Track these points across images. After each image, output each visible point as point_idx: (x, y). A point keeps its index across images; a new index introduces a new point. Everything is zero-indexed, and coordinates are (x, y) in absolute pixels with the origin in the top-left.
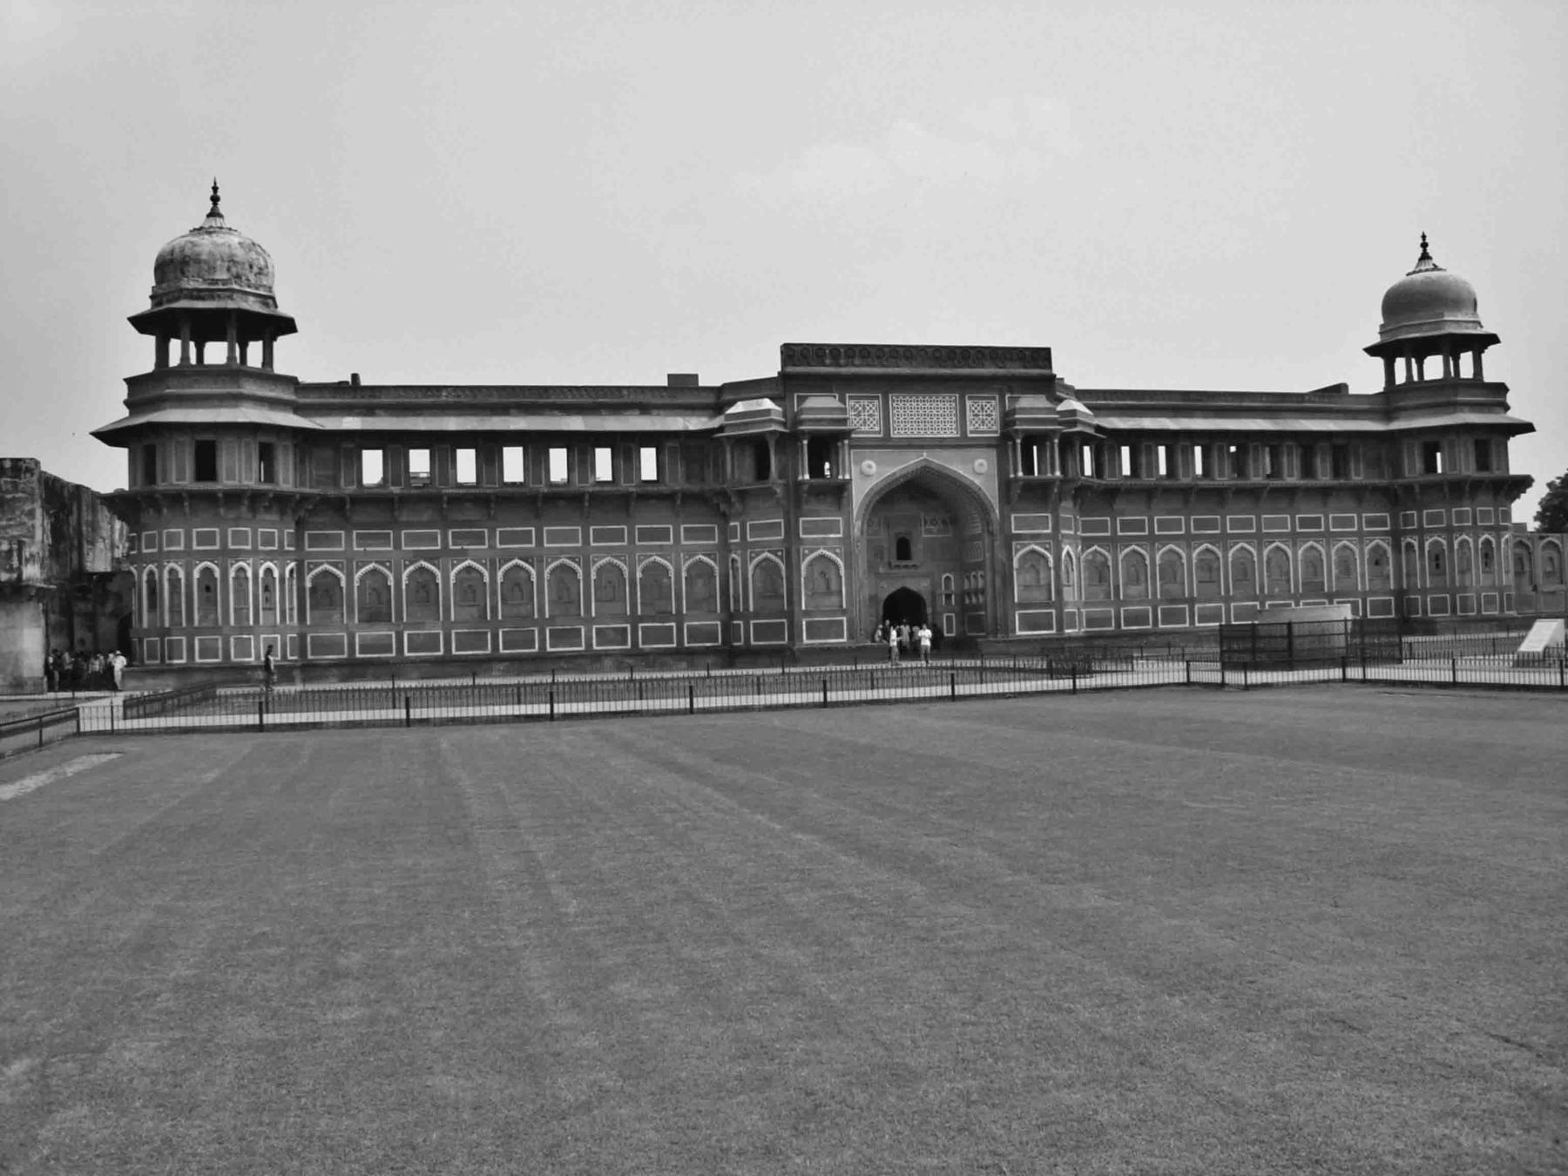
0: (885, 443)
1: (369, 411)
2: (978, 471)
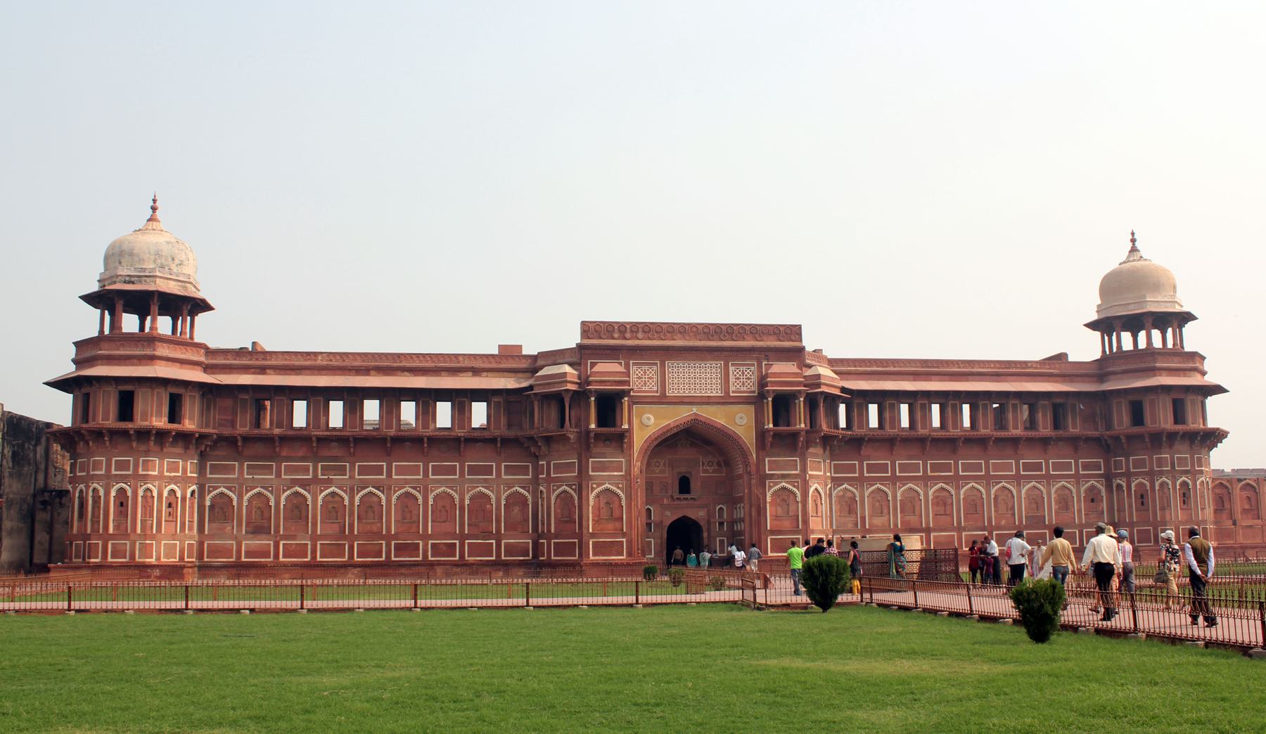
0: (662, 399)
1: (262, 370)
2: (740, 423)
